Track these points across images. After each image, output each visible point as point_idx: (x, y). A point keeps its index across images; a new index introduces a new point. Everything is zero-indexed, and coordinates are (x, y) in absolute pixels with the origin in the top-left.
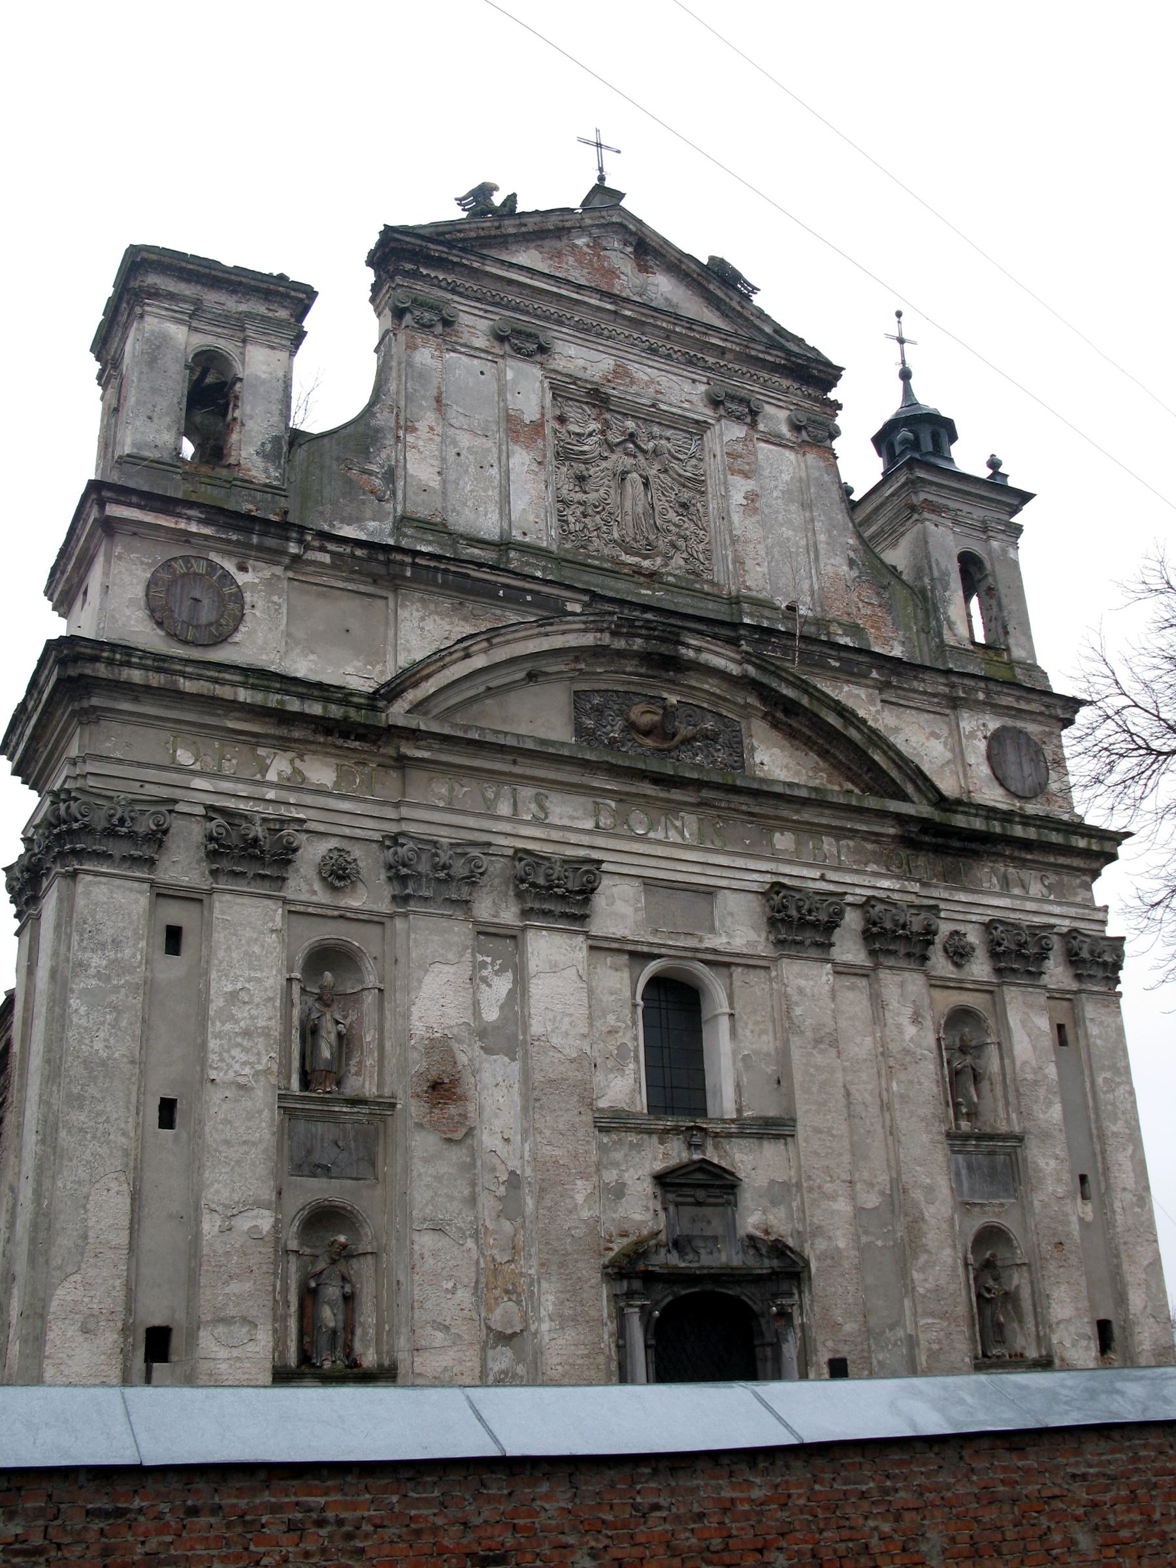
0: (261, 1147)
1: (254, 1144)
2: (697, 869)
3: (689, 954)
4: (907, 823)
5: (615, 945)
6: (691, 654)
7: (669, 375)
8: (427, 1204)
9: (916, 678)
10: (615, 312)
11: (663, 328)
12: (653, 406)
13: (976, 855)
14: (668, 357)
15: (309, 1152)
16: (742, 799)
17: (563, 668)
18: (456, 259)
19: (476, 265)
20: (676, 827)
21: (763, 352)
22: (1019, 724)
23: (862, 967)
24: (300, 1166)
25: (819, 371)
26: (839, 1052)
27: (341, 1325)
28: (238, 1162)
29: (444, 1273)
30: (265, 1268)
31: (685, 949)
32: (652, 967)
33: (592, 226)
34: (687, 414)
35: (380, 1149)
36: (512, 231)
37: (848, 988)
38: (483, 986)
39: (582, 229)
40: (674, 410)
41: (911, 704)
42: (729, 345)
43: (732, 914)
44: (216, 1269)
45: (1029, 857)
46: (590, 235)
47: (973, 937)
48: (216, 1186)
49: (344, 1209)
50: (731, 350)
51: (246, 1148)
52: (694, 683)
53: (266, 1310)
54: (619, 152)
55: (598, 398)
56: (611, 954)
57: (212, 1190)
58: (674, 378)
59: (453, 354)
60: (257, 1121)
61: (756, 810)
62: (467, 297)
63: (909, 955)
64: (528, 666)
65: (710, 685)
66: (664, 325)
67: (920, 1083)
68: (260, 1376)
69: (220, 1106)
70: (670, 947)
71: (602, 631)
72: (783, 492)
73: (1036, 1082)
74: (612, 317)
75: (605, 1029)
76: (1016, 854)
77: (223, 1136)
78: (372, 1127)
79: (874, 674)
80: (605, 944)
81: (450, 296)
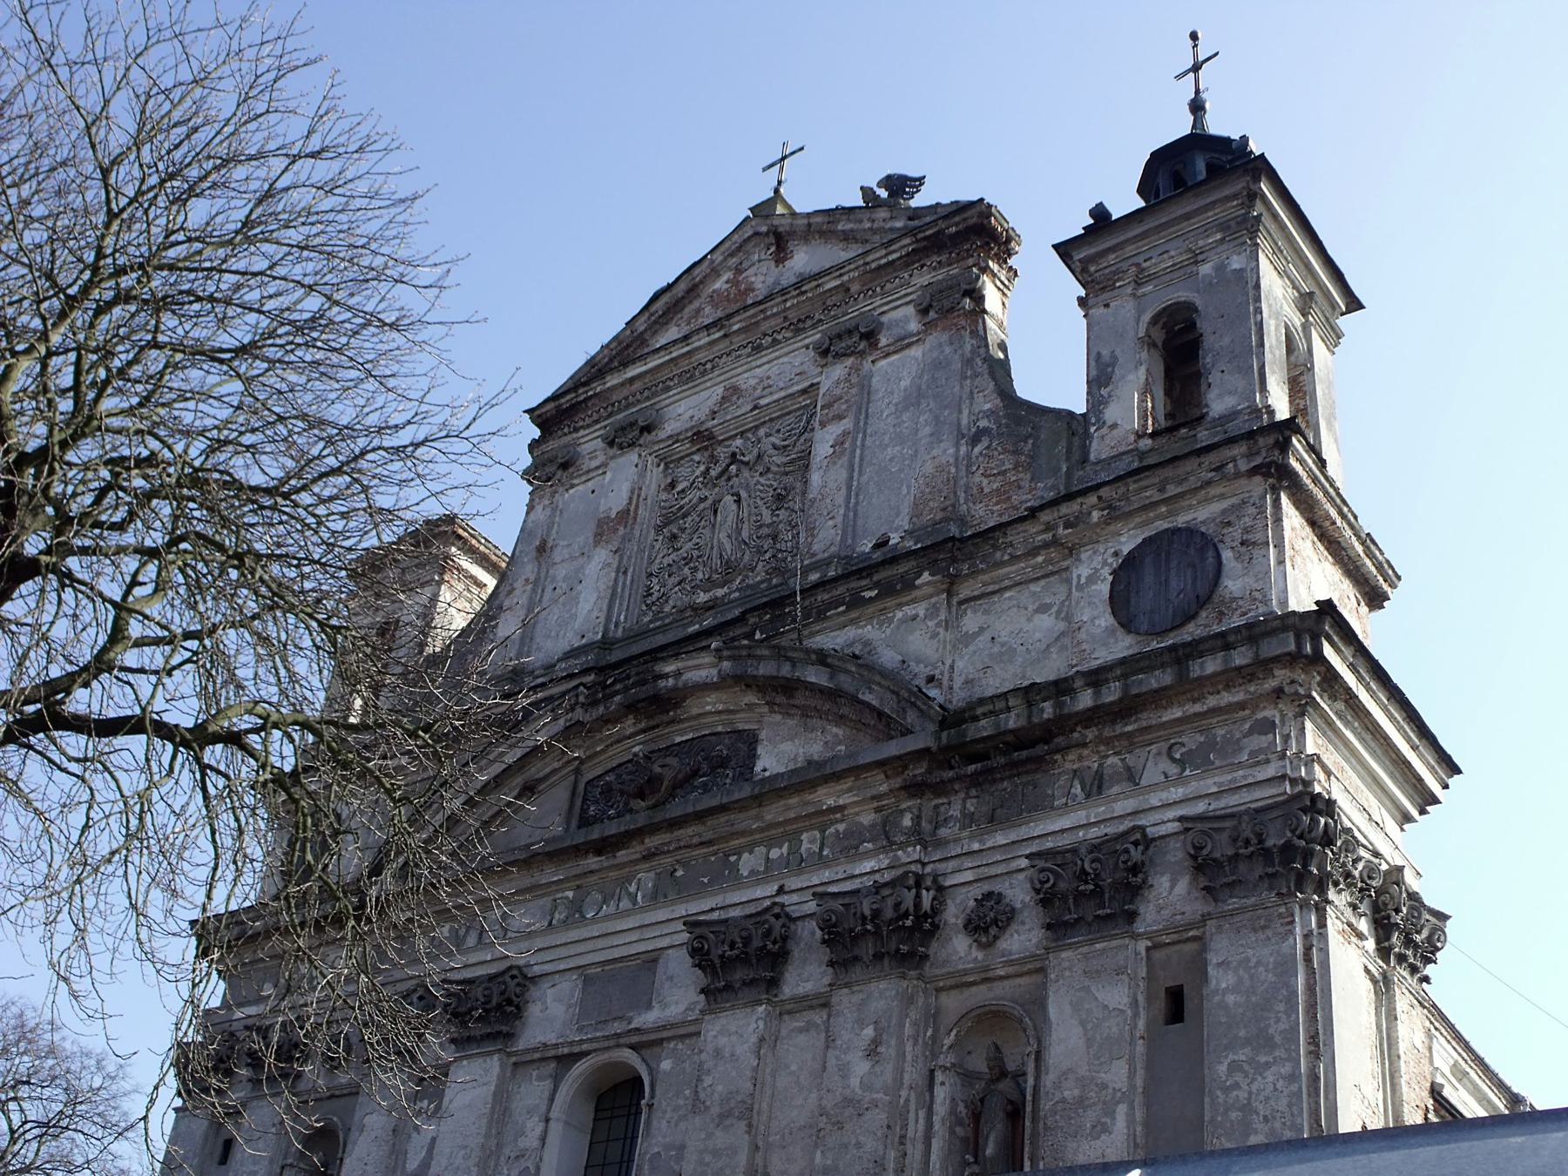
2: (634, 937)
3: (612, 1043)
4: (905, 768)
5: (537, 1056)
6: (671, 681)
7: (781, 360)
9: (995, 547)
10: (725, 336)
11: (774, 315)
12: (755, 407)
13: (1040, 763)
14: (775, 342)
16: (690, 831)
17: (556, 765)
18: (582, 398)
19: (598, 390)
20: (629, 894)
21: (887, 255)
22: (1181, 520)
23: (818, 996)
25: (957, 224)
26: (750, 1126)
31: (607, 1038)
32: (580, 1068)
33: (725, 259)
34: (790, 391)
36: (642, 328)
37: (801, 1030)
38: (414, 1135)
39: (715, 272)
40: (776, 397)
41: (1007, 583)
42: (845, 278)
43: (671, 978)
45: (1129, 728)
46: (730, 269)
47: (1018, 893)
50: (851, 280)
52: (695, 711)
54: (802, 149)
55: (702, 437)
56: (535, 1066)
58: (785, 359)
59: (571, 491)
61: (708, 836)
62: (589, 426)
63: (878, 957)
64: (518, 781)
65: (712, 702)
66: (775, 310)
67: (859, 1145)
70: (590, 1040)
71: (572, 709)
72: (896, 405)
73: (1081, 1102)
74: (727, 341)
75: (513, 1155)
76: (1107, 732)
79: (926, 576)
80: (528, 1057)
81: (575, 435)
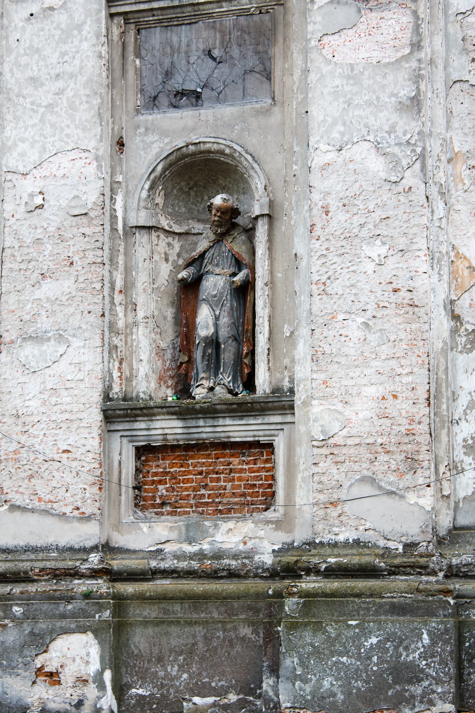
0: (82, 79)
1: (72, 76)
8: (335, 123)
15: (168, 74)
24: (155, 98)
27: (224, 333)
28: (50, 106)
29: (364, 233)
30: (91, 256)
35: (277, 51)
44: (23, 266)
48: (22, 147)
49: (222, 152)
51: (60, 84)
53: (92, 318)
57: (15, 154)
60: (76, 42)
68: (84, 415)
69: (23, 29)
77: (29, 73)
78: (266, 17)
